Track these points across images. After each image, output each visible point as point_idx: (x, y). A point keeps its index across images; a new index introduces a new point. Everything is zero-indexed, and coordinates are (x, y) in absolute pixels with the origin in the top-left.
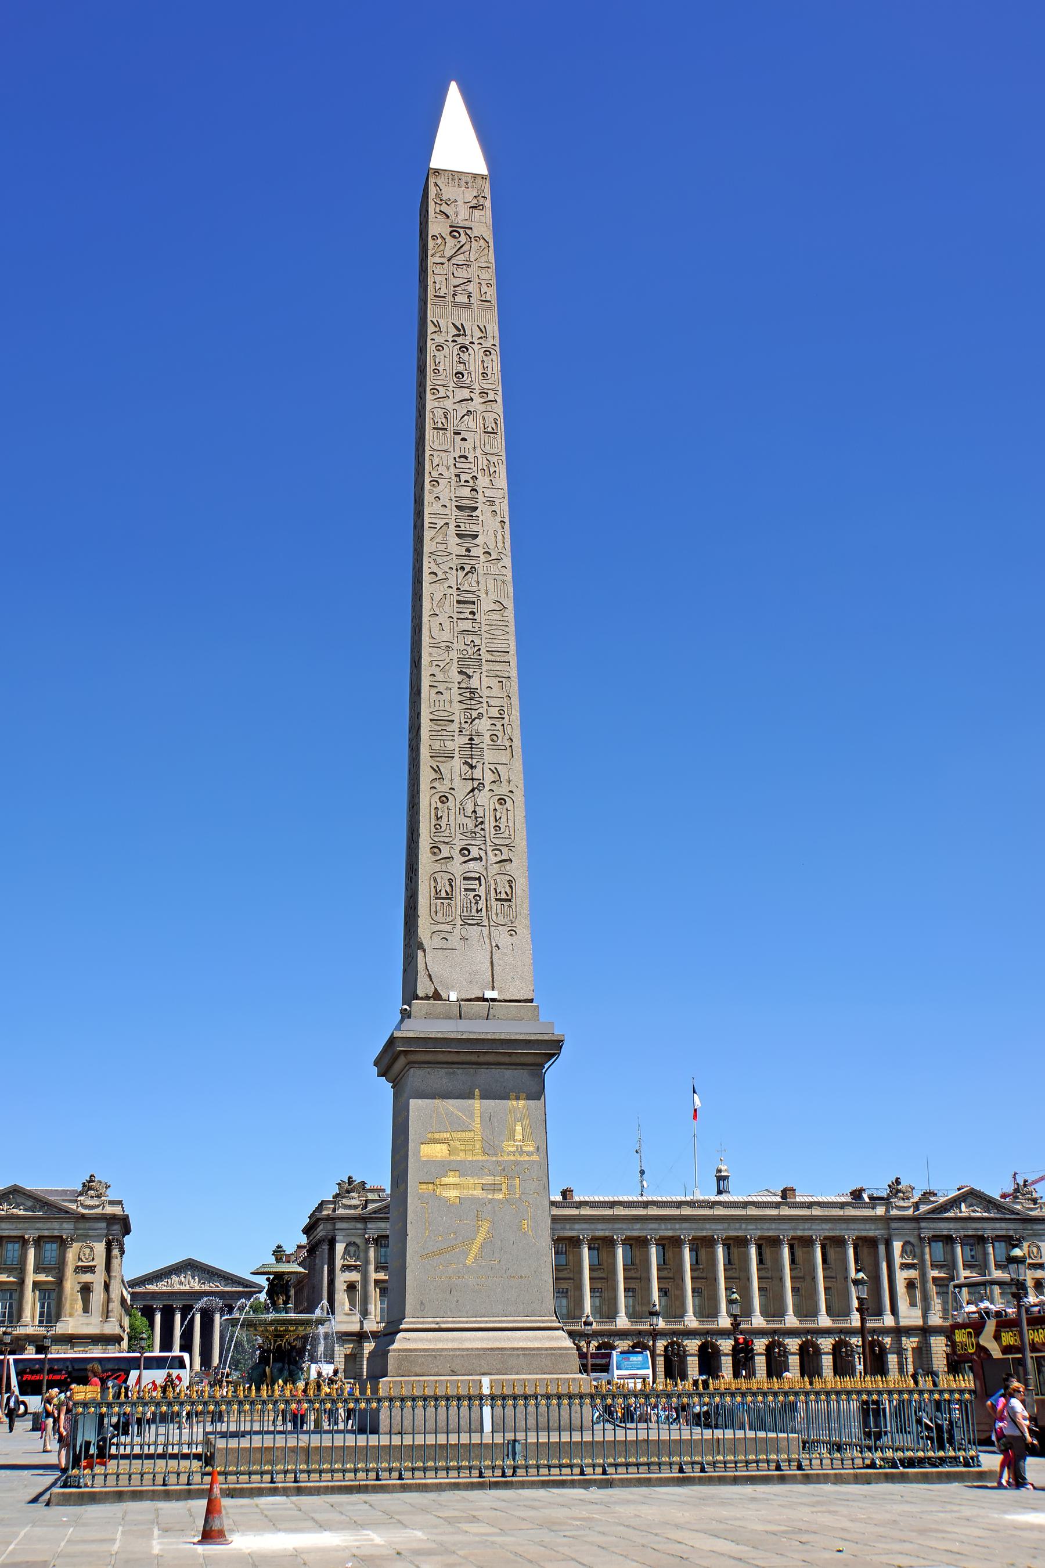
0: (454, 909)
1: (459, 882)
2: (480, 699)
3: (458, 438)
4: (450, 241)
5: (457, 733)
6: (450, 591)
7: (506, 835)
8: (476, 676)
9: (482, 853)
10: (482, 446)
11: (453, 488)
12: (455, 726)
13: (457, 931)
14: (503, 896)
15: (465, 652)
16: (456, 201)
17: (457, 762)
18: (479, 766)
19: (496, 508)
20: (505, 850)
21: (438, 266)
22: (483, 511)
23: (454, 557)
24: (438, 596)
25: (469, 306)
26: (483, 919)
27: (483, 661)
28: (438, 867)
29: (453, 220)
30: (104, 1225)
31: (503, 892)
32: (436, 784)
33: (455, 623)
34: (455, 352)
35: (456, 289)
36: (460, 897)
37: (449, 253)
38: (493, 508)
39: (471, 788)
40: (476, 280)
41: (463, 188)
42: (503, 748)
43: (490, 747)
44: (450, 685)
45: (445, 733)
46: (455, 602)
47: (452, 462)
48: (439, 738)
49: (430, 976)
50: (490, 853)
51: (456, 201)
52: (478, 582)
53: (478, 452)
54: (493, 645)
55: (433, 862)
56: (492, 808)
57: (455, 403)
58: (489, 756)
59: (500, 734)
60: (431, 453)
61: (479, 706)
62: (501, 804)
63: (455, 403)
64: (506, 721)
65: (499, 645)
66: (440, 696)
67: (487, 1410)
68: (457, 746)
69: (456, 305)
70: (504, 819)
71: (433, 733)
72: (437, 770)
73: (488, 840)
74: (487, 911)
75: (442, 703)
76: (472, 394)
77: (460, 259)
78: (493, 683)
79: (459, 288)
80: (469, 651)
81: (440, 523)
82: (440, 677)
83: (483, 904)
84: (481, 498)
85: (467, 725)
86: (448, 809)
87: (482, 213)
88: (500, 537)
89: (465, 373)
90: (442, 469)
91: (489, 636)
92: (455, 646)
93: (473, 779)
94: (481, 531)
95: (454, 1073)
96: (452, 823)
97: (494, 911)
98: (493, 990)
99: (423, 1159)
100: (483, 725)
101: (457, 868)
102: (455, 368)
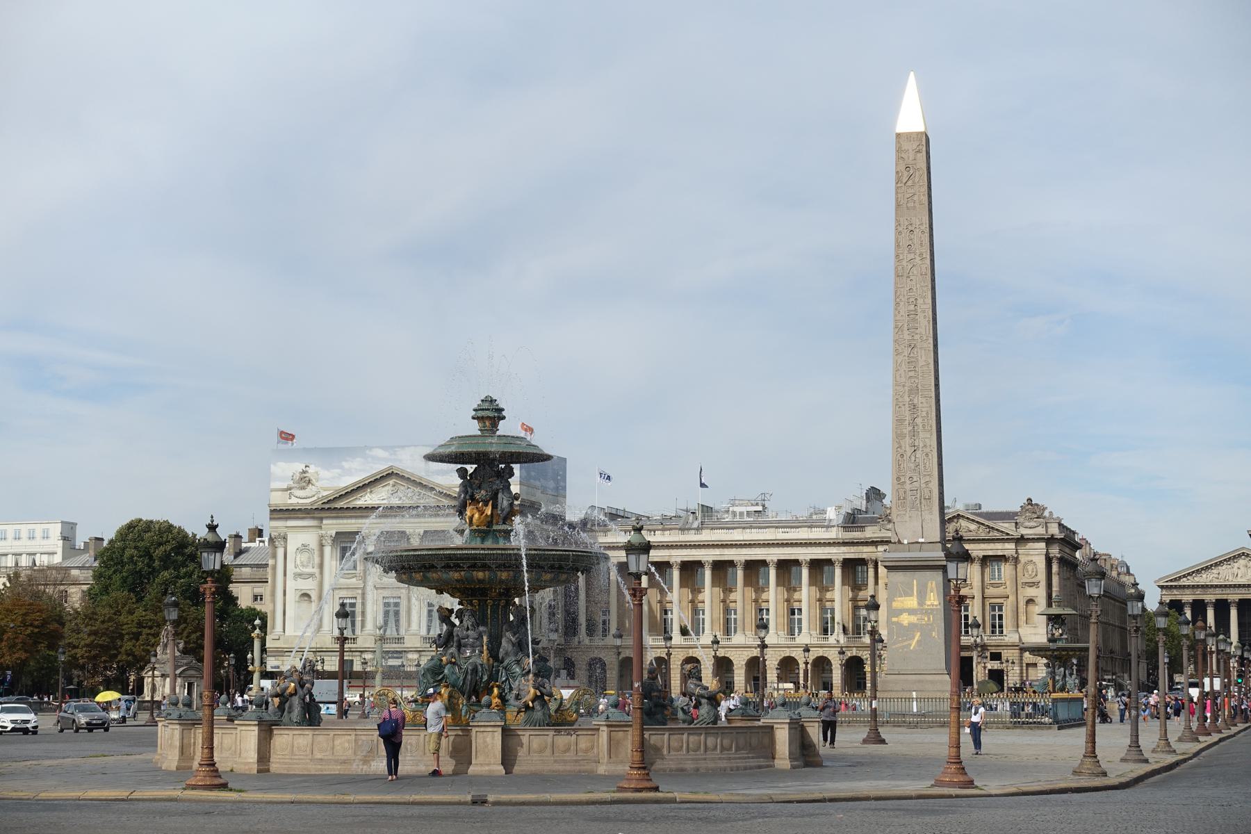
1: (909, 493)
22: (920, 317)
30: (1043, 545)
32: (899, 449)
40: (918, 193)
51: (908, 150)
53: (918, 286)
58: (921, 435)
64: (929, 418)
67: (915, 703)
69: (907, 207)
76: (916, 256)
77: (910, 183)
78: (924, 400)
81: (901, 324)
82: (900, 400)
84: (919, 310)
88: (927, 328)
90: (901, 297)
92: (907, 384)
100: (919, 421)
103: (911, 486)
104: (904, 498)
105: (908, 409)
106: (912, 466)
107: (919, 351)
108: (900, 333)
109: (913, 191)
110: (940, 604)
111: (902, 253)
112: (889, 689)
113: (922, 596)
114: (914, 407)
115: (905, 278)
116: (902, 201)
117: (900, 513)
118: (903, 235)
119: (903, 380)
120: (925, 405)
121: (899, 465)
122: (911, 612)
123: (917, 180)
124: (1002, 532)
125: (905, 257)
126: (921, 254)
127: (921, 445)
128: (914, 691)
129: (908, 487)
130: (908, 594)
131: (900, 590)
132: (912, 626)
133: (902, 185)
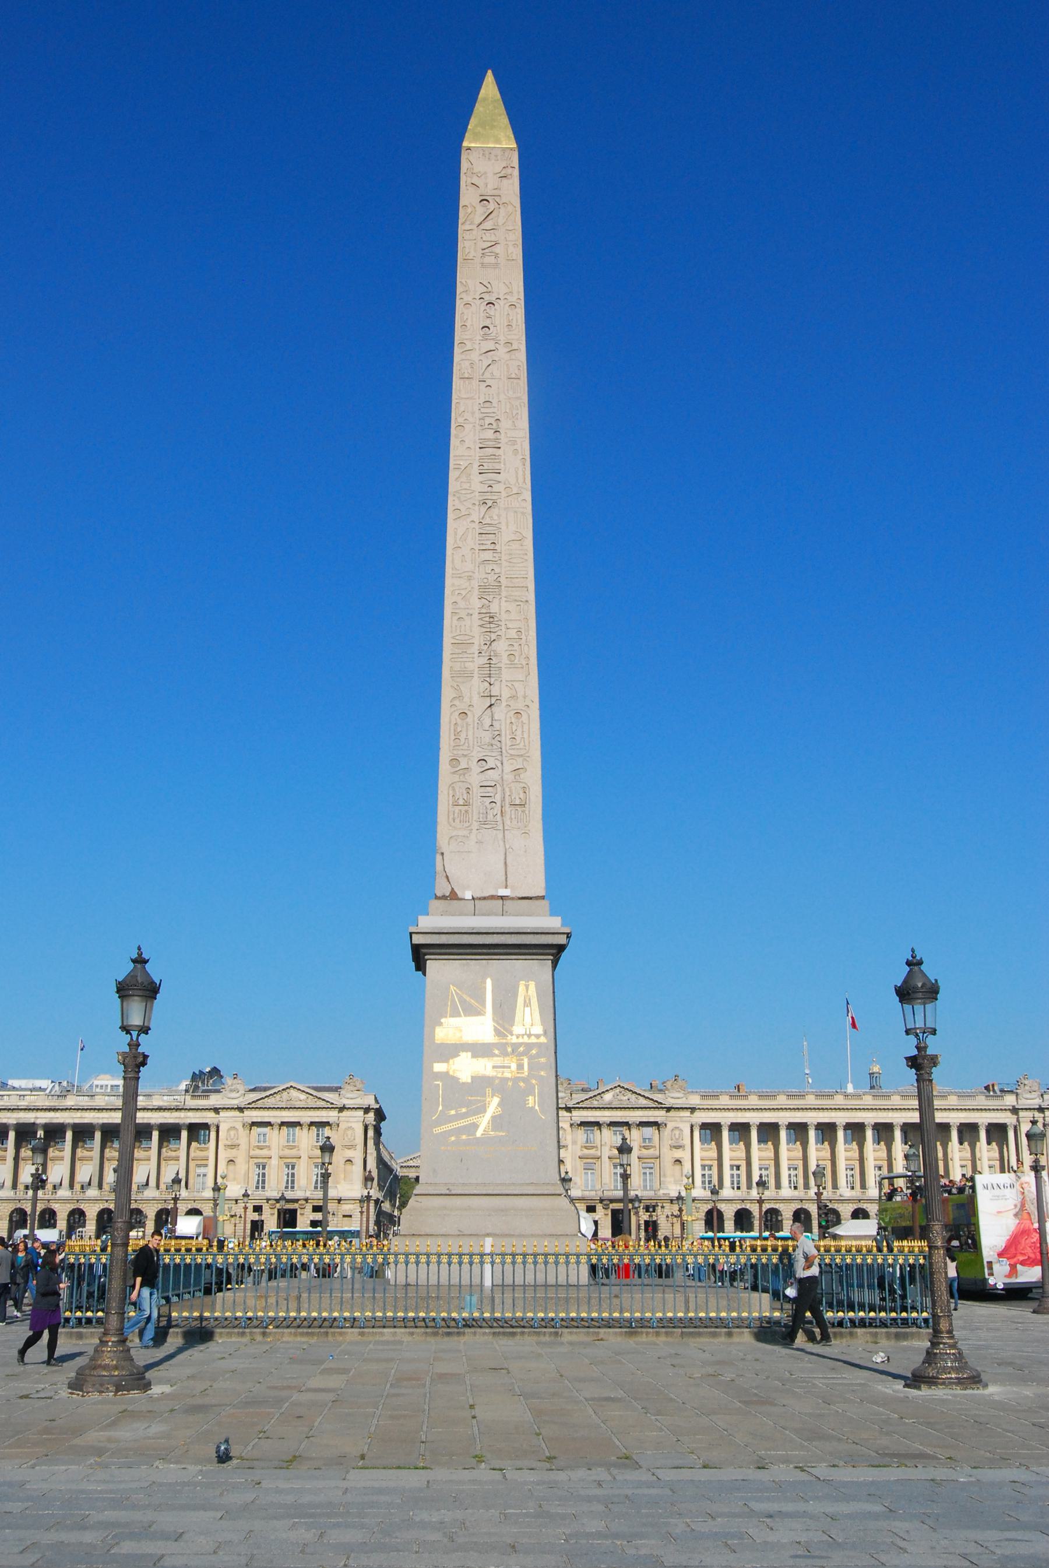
0: (470, 816)
1: (477, 791)
2: (499, 623)
6: (473, 525)
8: (496, 601)
9: (499, 765)
10: (506, 392)
11: (477, 431)
15: (485, 581)
16: (485, 173)
17: (476, 681)
18: (497, 684)
19: (518, 447)
20: (520, 760)
21: (468, 232)
23: (477, 494)
25: (496, 266)
26: (498, 823)
27: (503, 587)
28: (456, 778)
29: (482, 191)
31: (517, 798)
32: (456, 702)
33: (477, 553)
34: (482, 308)
35: (484, 251)
36: (477, 802)
38: (515, 447)
39: (489, 705)
41: (493, 161)
42: (520, 666)
43: (508, 666)
44: (471, 612)
45: (466, 655)
46: (477, 535)
47: (476, 408)
48: (461, 660)
49: (447, 877)
50: (505, 762)
52: (499, 516)
53: (502, 397)
54: (512, 572)
56: (508, 722)
57: (481, 355)
58: (506, 675)
60: (457, 401)
61: (497, 629)
62: (517, 718)
63: (481, 355)
64: (523, 641)
65: (518, 572)
67: (488, 1267)
68: (477, 667)
70: (519, 733)
71: (454, 656)
72: (457, 689)
73: (504, 751)
74: (502, 816)
75: (463, 628)
77: (488, 225)
78: (512, 607)
79: (487, 251)
80: (490, 579)
81: (463, 464)
82: (462, 604)
83: (498, 810)
85: (486, 647)
86: (467, 724)
87: (510, 181)
91: (508, 564)
93: (491, 696)
94: (503, 469)
97: (508, 817)
98: (506, 888)
99: (436, 1042)
100: (501, 646)
101: (475, 778)
102: (482, 322)
103: (482, 777)
108: (464, 479)
109: (493, 238)
110: (545, 1033)
111: (471, 340)
112: (428, 1231)
113: (505, 1015)
114: (490, 619)
115: (475, 383)
121: (457, 734)
122: (479, 1050)
123: (501, 221)
124: (328, 1102)
125: (477, 347)
128: (488, 1235)
129: (475, 778)
130: (473, 1010)
131: (453, 1001)
132: (481, 1083)
133: (474, 227)
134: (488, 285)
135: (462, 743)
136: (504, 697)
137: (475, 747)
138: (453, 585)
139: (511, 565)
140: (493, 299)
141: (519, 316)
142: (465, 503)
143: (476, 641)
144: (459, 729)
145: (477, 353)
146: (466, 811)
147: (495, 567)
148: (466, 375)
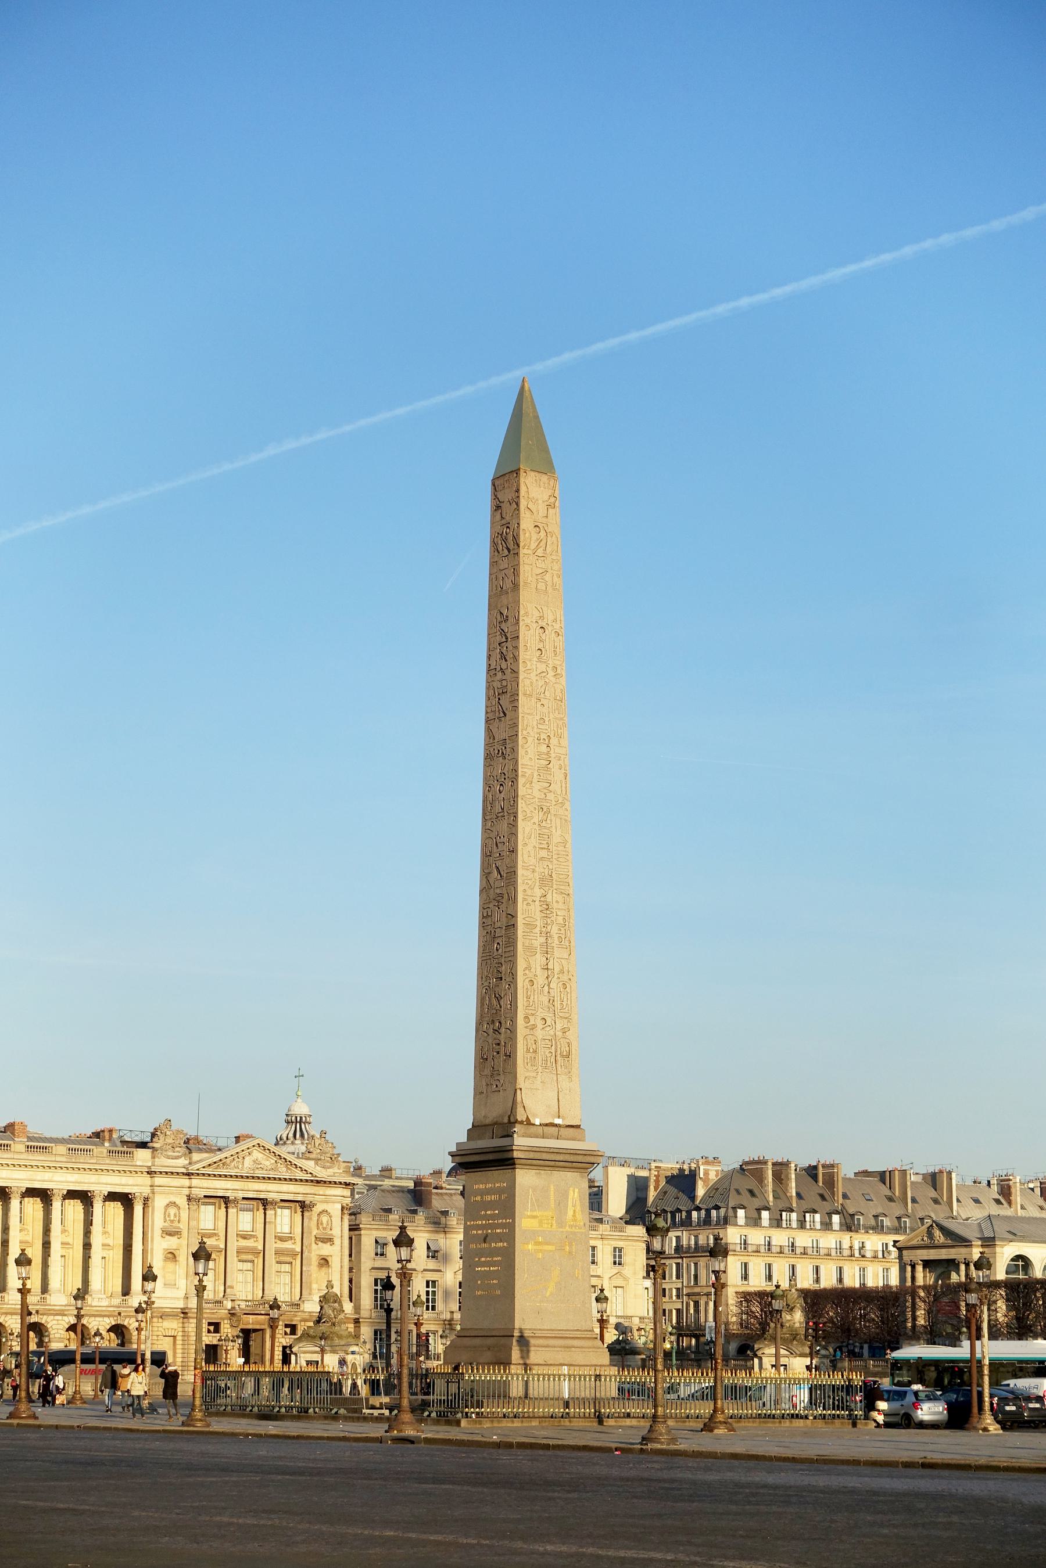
3: (539, 704)
4: (534, 537)
5: (538, 935)
7: (566, 1010)
8: (550, 891)
9: (553, 1024)
12: (537, 930)
13: (539, 1078)
14: (565, 1053)
15: (543, 874)
18: (552, 959)
24: (527, 830)
28: (528, 1031)
32: (527, 972)
36: (540, 1051)
37: (533, 545)
47: (535, 723)
52: (551, 820)
53: (551, 716)
55: (526, 1027)
56: (559, 990)
58: (557, 953)
59: (563, 937)
60: (523, 715)
66: (530, 907)
70: (565, 999)
71: (525, 934)
77: (540, 552)
78: (560, 898)
81: (529, 772)
82: (529, 892)
84: (553, 755)
89: (543, 649)
90: (529, 729)
92: (537, 869)
95: (540, 1173)
96: (536, 1000)
97: (559, 1063)
104: (535, 1052)
105: (540, 909)
106: (545, 999)
107: (553, 818)
116: (530, 578)
117: (527, 1074)
118: (532, 631)
119: (533, 861)
120: (561, 906)
121: (528, 997)
126: (555, 668)
127: (557, 969)
129: (539, 1034)
134: (541, 611)
135: (531, 1004)
136: (556, 972)
137: (540, 1009)
138: (523, 875)
139: (559, 863)
140: (544, 625)
141: (561, 644)
142: (529, 806)
143: (538, 924)
144: (529, 994)
145: (535, 673)
146: (535, 1058)
147: (549, 863)
148: (528, 693)
